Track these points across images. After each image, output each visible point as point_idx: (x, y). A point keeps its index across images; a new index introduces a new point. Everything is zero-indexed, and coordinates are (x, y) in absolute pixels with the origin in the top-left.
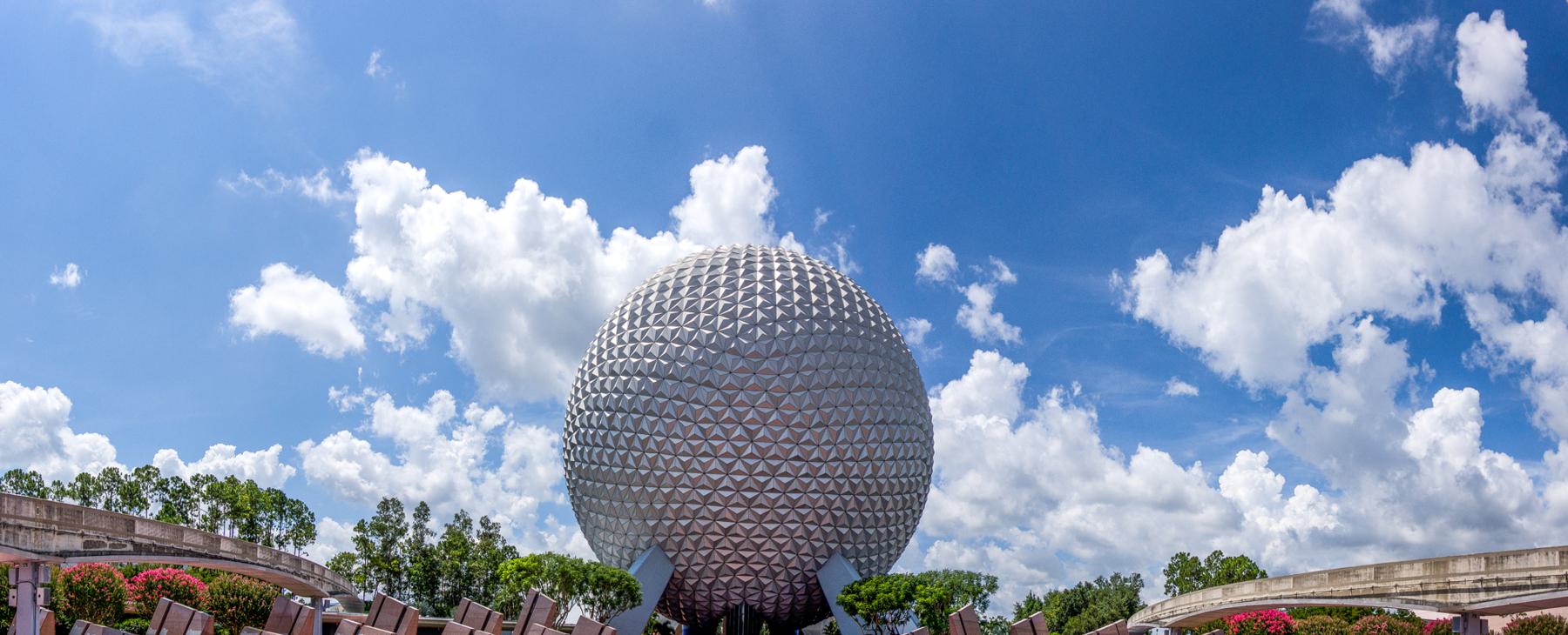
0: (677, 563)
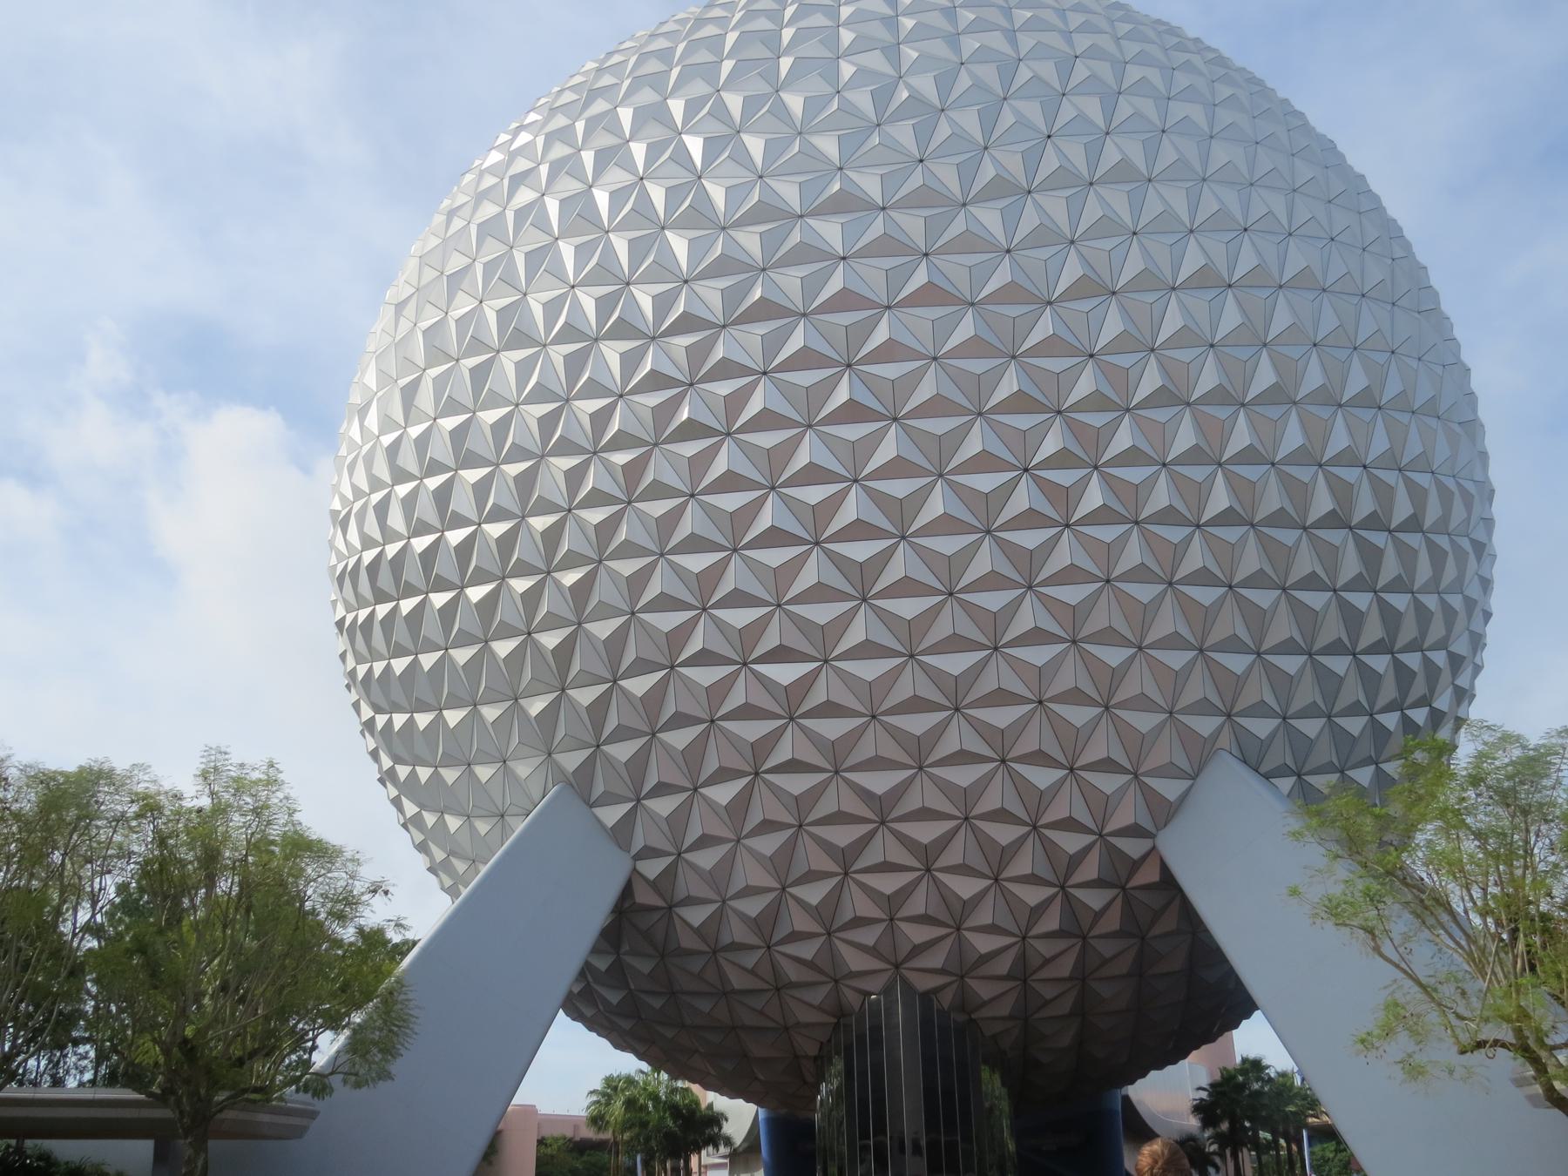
0: (638, 844)
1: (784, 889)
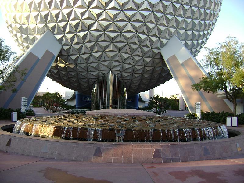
0: (63, 43)
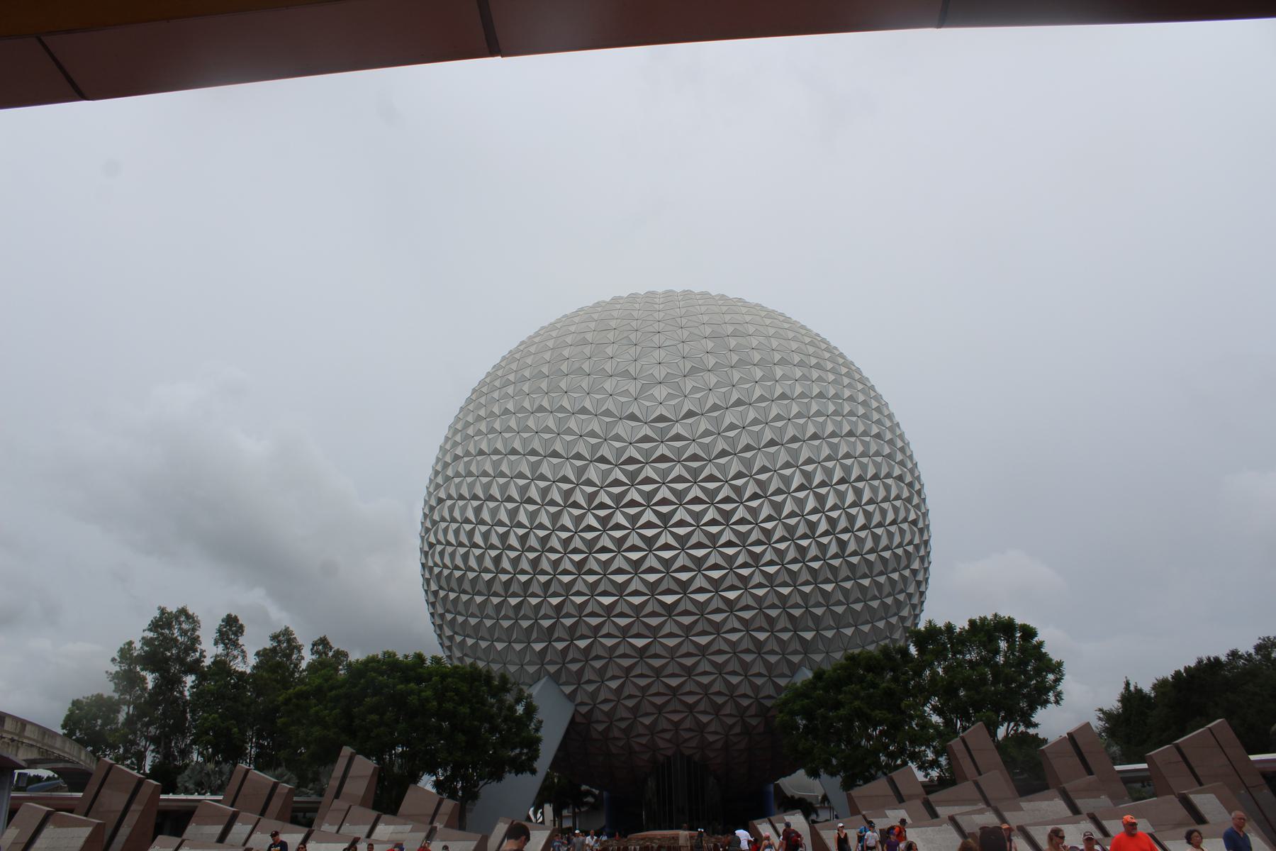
0: (578, 700)
1: (635, 718)
